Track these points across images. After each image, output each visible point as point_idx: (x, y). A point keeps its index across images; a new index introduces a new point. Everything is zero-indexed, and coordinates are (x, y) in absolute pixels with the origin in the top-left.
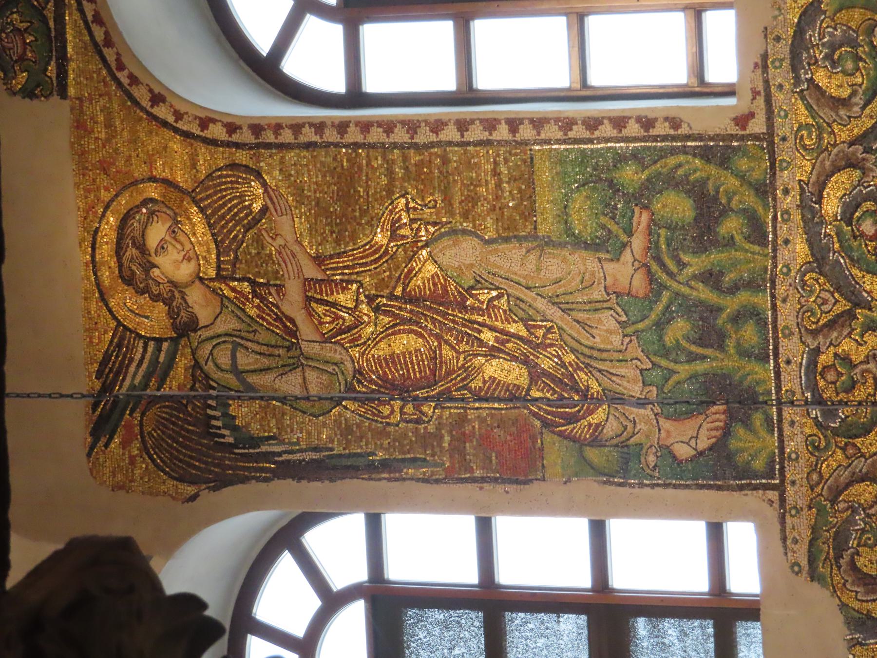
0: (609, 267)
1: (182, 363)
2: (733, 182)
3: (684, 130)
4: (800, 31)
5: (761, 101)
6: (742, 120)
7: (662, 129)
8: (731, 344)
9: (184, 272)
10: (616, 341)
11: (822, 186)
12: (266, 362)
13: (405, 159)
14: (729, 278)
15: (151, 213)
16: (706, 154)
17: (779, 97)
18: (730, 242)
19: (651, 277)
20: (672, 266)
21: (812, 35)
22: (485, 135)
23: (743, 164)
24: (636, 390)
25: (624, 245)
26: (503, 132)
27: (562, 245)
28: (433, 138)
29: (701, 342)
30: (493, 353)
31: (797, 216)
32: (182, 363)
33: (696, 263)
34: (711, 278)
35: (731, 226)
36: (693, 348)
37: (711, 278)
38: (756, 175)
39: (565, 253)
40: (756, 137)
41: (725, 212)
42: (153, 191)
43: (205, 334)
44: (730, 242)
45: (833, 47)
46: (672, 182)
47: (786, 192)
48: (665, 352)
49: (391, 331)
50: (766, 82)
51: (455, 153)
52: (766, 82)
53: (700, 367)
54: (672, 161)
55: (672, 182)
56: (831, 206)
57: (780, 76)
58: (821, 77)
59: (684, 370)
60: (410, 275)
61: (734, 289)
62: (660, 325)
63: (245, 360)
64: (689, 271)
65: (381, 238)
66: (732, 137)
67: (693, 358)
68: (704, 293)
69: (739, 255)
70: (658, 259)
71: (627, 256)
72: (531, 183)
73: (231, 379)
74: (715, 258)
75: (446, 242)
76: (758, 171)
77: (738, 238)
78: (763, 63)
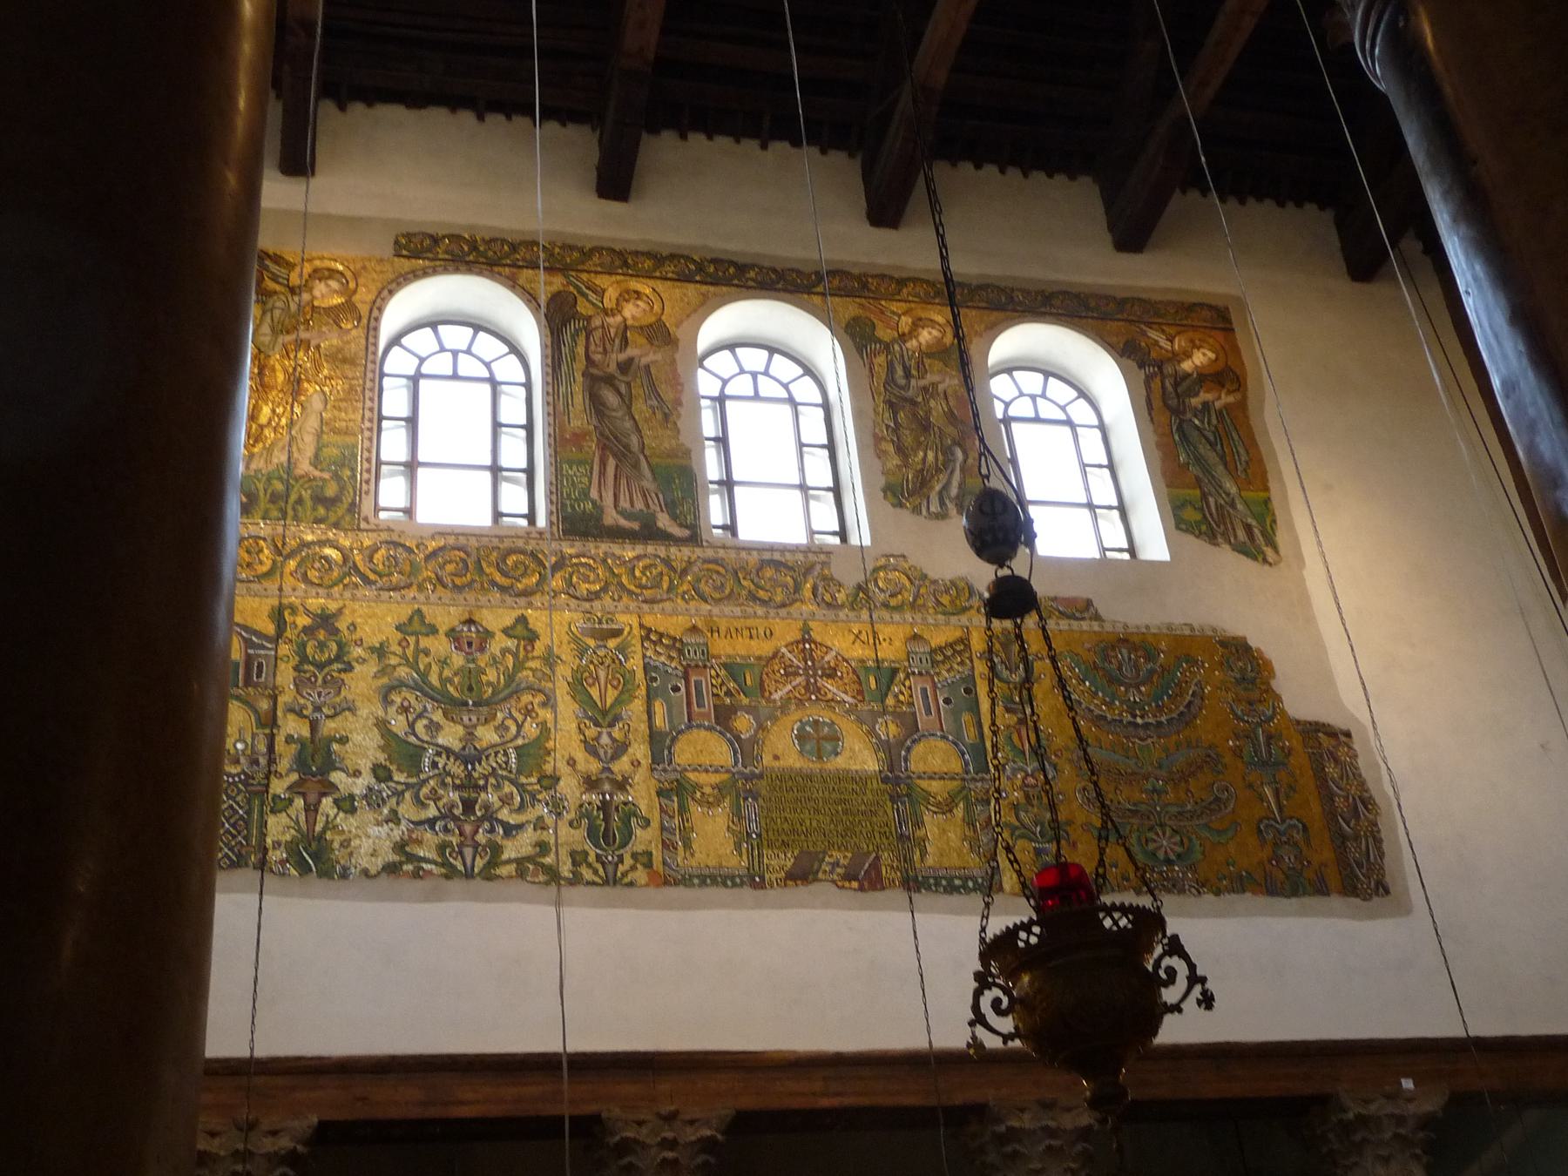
0: (308, 462)
1: (278, 288)
2: (340, 512)
3: (363, 495)
4: (403, 546)
5: (374, 527)
6: (366, 520)
7: (365, 487)
8: (272, 506)
9: (317, 293)
10: (275, 461)
11: (337, 548)
12: (276, 320)
13: (359, 385)
14: (300, 508)
15: (342, 283)
16: (353, 504)
17: (375, 535)
18: (314, 509)
19: (302, 477)
20: (306, 486)
21: (400, 550)
22: (366, 417)
23: (348, 518)
24: (253, 466)
25: (316, 468)
26: (368, 424)
27: (318, 442)
28: (367, 397)
29: (273, 494)
30: (274, 411)
31: (324, 538)
32: (278, 288)
33: (306, 495)
34: (300, 501)
35: (321, 511)
36: (269, 491)
37: (300, 501)
38: (343, 523)
39: (315, 443)
40: (359, 525)
41: (328, 509)
42: (352, 285)
43: (290, 299)
44: (314, 509)
45: (395, 558)
46: (342, 489)
47: (335, 534)
48: (269, 479)
49: (285, 371)
50: (381, 530)
51: (360, 405)
52: (381, 530)
53: (262, 493)
54: (351, 491)
55: (342, 489)
56: (328, 551)
57: (384, 536)
58: (382, 552)
59: (261, 486)
60: (309, 381)
61: (294, 509)
62: (280, 478)
63: (277, 313)
64: (303, 493)
65: (326, 372)
66: (359, 515)
67: (265, 490)
68: (293, 497)
69: (309, 513)
70: (310, 480)
71: (311, 468)
72: (346, 433)
73: (269, 306)
74: (309, 503)
75: (323, 397)
76: (345, 524)
77: (315, 514)
78: (389, 530)
